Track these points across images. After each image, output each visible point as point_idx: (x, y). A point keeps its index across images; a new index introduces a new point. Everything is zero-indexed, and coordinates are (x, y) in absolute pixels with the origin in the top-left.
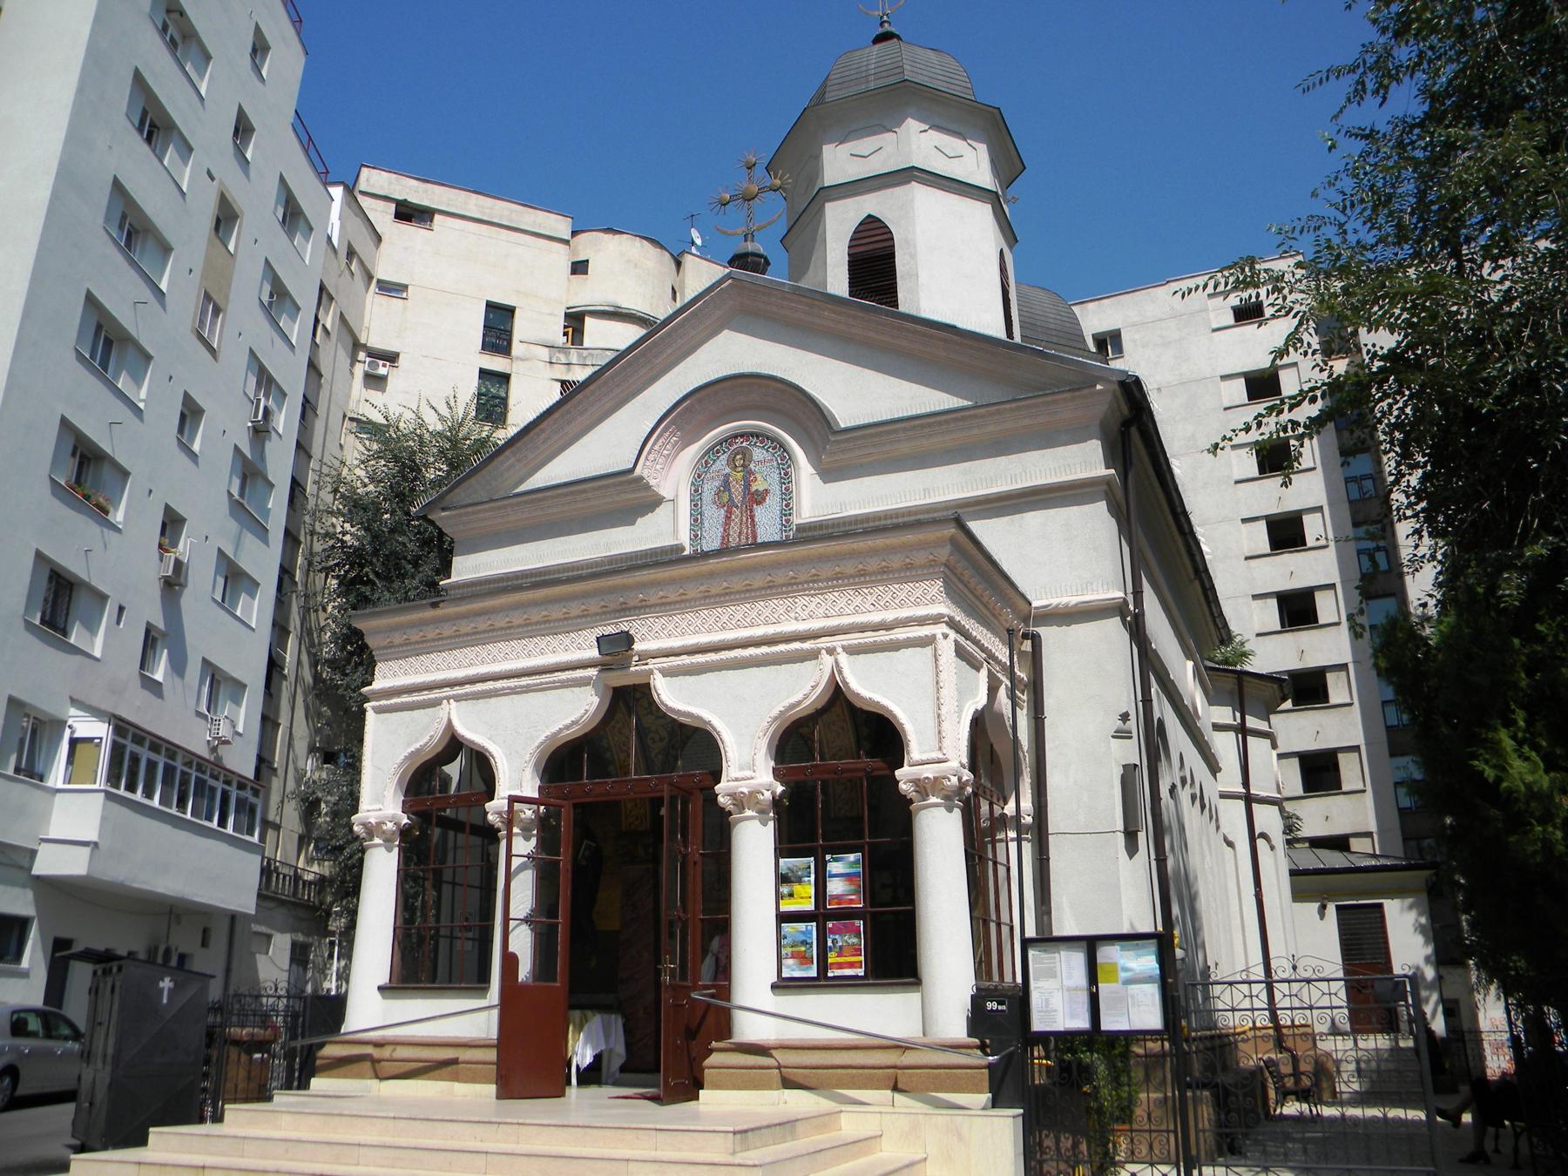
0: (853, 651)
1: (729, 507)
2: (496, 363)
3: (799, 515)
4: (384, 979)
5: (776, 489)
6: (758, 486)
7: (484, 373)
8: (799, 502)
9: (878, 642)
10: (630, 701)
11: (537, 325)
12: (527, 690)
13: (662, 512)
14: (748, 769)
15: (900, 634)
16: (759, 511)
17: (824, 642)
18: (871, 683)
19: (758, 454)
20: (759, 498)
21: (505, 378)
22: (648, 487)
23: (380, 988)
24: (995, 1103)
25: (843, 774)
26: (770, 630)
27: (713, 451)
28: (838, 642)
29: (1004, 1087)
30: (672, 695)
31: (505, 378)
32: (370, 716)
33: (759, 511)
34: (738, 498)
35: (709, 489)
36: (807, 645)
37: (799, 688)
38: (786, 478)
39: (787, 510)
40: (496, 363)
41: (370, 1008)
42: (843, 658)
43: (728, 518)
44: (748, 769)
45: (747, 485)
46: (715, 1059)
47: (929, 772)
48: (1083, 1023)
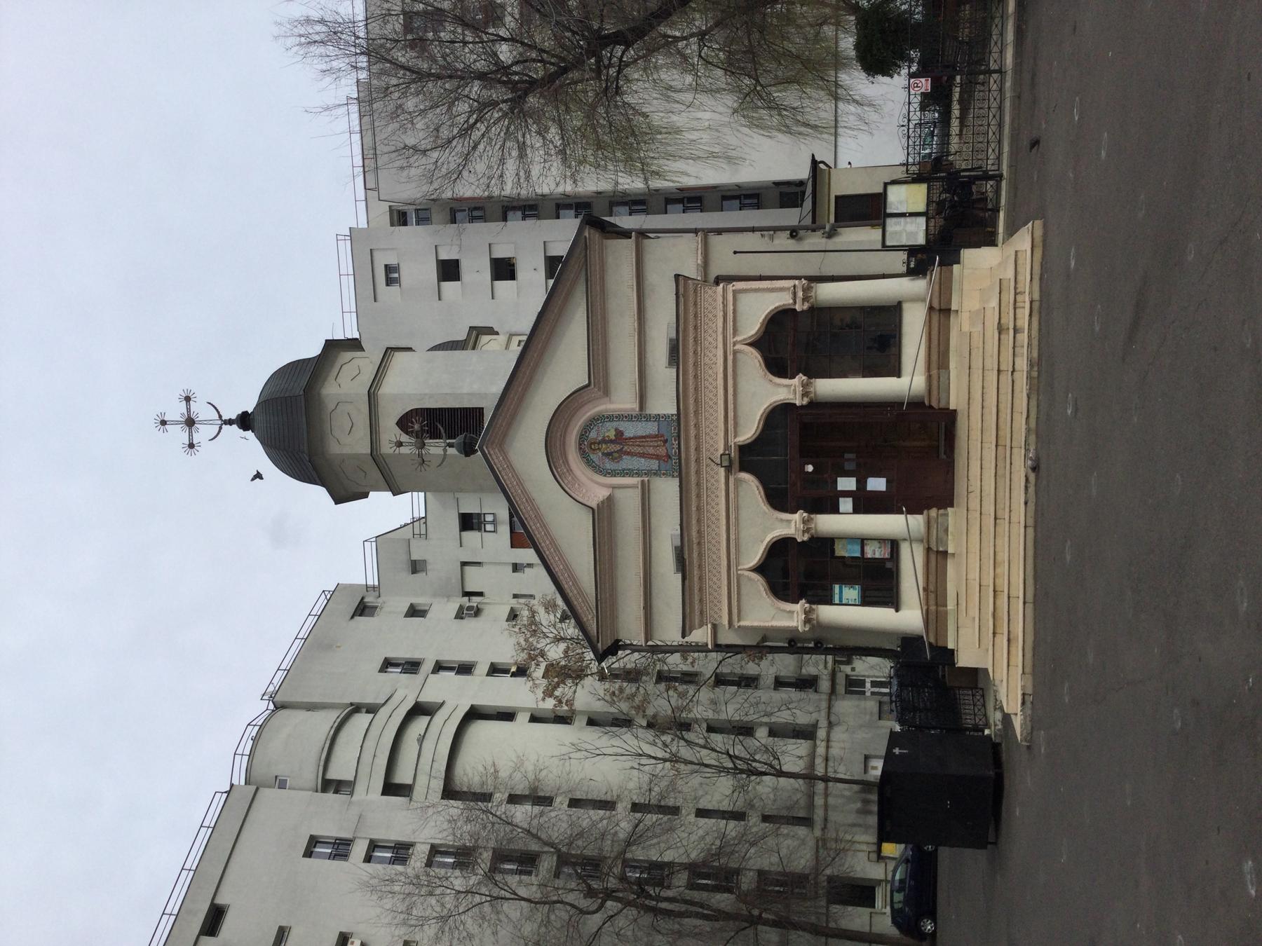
0: (735, 334)
1: (621, 452)
2: (359, 849)
3: (633, 410)
4: (892, 611)
5: (615, 424)
6: (612, 434)
7: (368, 859)
8: (625, 410)
9: (733, 321)
10: (749, 458)
11: (330, 817)
12: (737, 519)
13: (619, 494)
14: (788, 390)
15: (730, 307)
16: (627, 434)
17: (730, 349)
18: (752, 325)
19: (593, 435)
20: (619, 434)
21: (374, 845)
22: (603, 502)
23: (897, 611)
24: (958, 262)
25: (795, 341)
26: (721, 376)
27: (589, 463)
28: (730, 340)
29: (951, 258)
30: (749, 432)
31: (374, 845)
32: (742, 623)
33: (629, 433)
34: (618, 447)
35: (609, 465)
36: (730, 358)
37: (753, 360)
38: (610, 418)
39: (629, 418)
40: (359, 849)
41: (908, 617)
42: (738, 338)
43: (628, 453)
44: (788, 390)
45: (611, 441)
46: (934, 404)
47: (800, 294)
48: (922, 220)
